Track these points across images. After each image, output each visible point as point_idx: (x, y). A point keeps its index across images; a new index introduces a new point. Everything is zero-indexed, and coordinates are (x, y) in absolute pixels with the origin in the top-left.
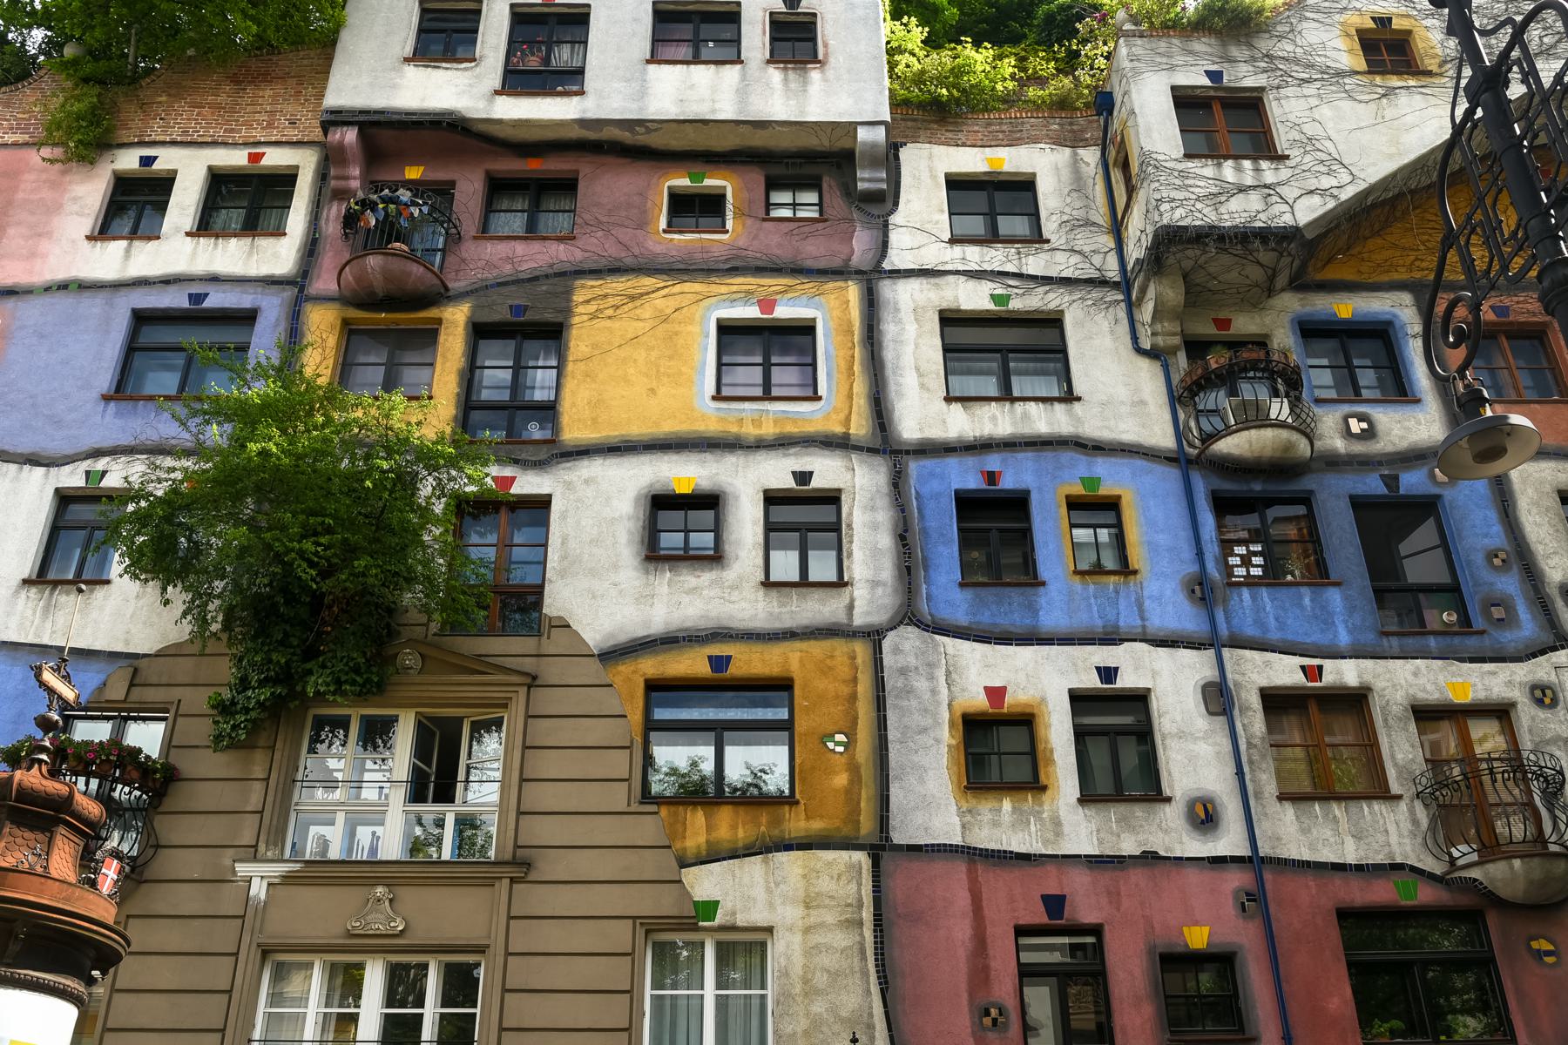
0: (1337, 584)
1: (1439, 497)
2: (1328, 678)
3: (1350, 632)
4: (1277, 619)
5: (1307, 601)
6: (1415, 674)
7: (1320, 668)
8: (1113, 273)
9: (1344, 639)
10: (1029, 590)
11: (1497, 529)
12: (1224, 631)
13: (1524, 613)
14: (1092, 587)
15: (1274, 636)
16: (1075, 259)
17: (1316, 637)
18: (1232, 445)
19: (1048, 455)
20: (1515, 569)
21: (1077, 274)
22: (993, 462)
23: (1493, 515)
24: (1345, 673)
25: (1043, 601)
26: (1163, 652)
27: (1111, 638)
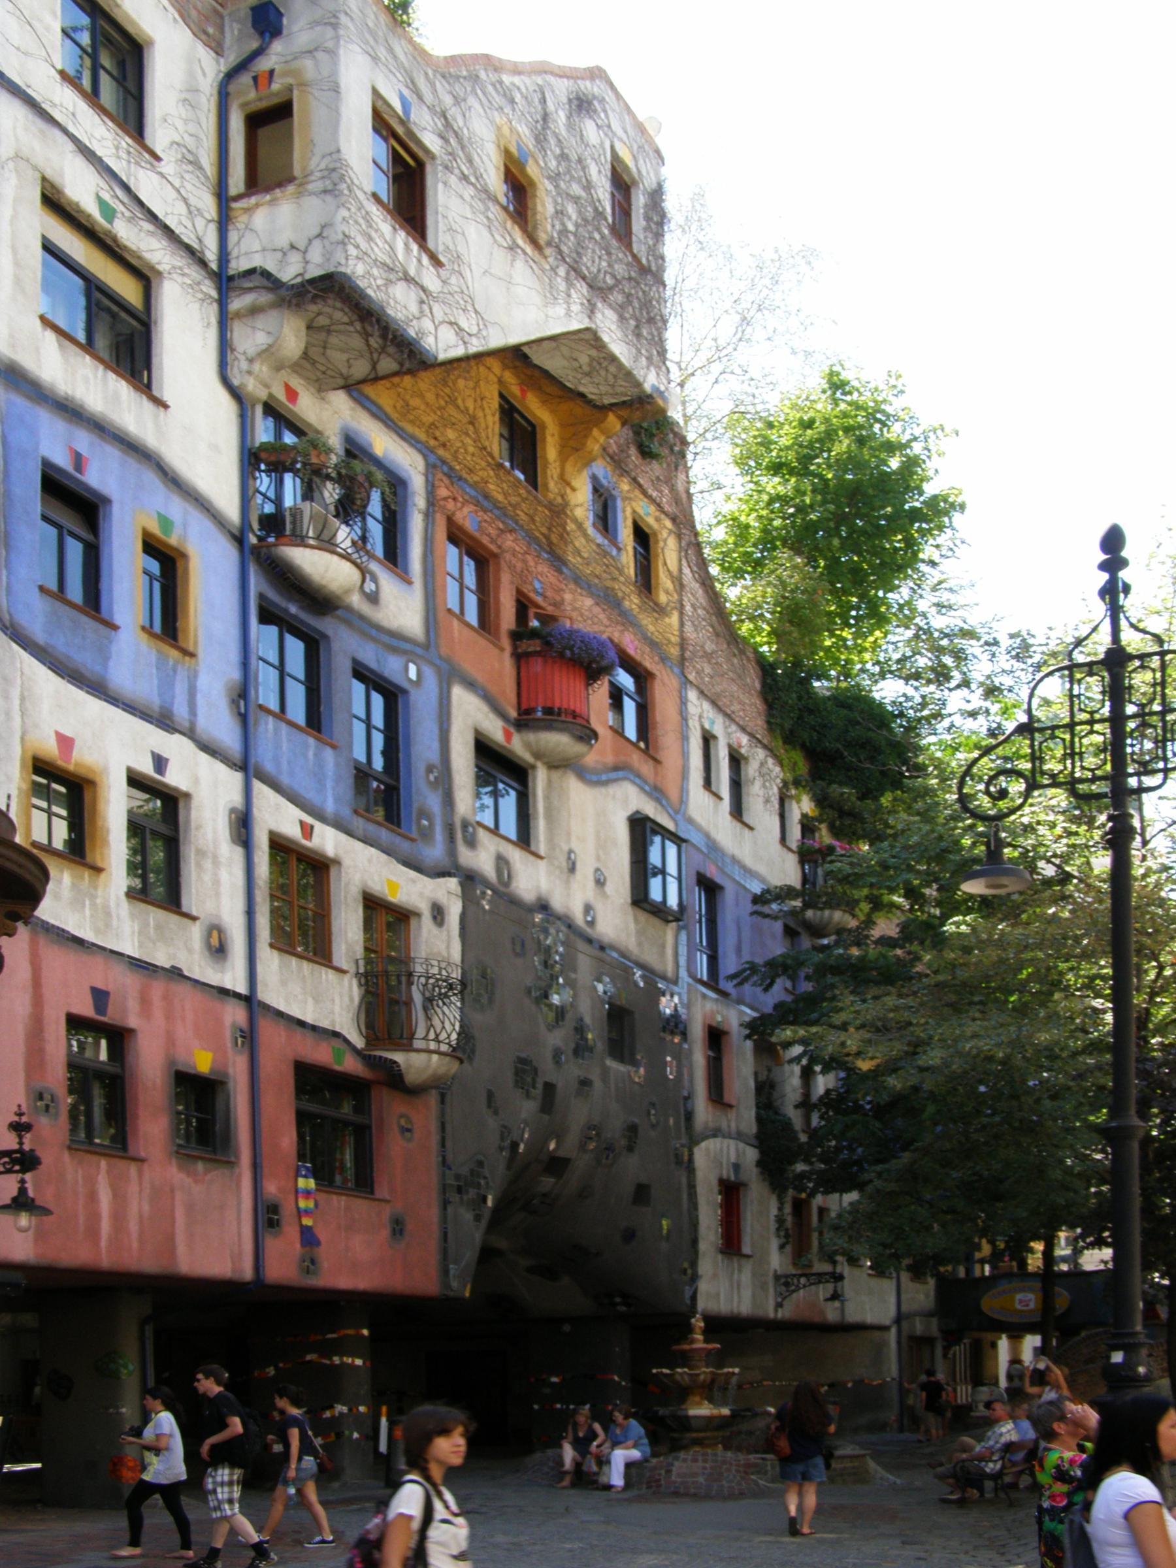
0: (334, 747)
1: (405, 692)
2: (315, 843)
3: (337, 800)
4: (289, 763)
5: (311, 754)
6: (370, 861)
7: (312, 827)
8: (211, 256)
9: (330, 807)
10: (103, 629)
11: (436, 745)
12: (252, 761)
13: (439, 835)
14: (154, 652)
15: (285, 780)
16: (181, 208)
17: (310, 795)
18: (310, 561)
19: (132, 463)
20: (440, 791)
21: (178, 230)
22: (84, 441)
23: (436, 731)
24: (327, 840)
25: (114, 648)
26: (204, 757)
27: (164, 721)
